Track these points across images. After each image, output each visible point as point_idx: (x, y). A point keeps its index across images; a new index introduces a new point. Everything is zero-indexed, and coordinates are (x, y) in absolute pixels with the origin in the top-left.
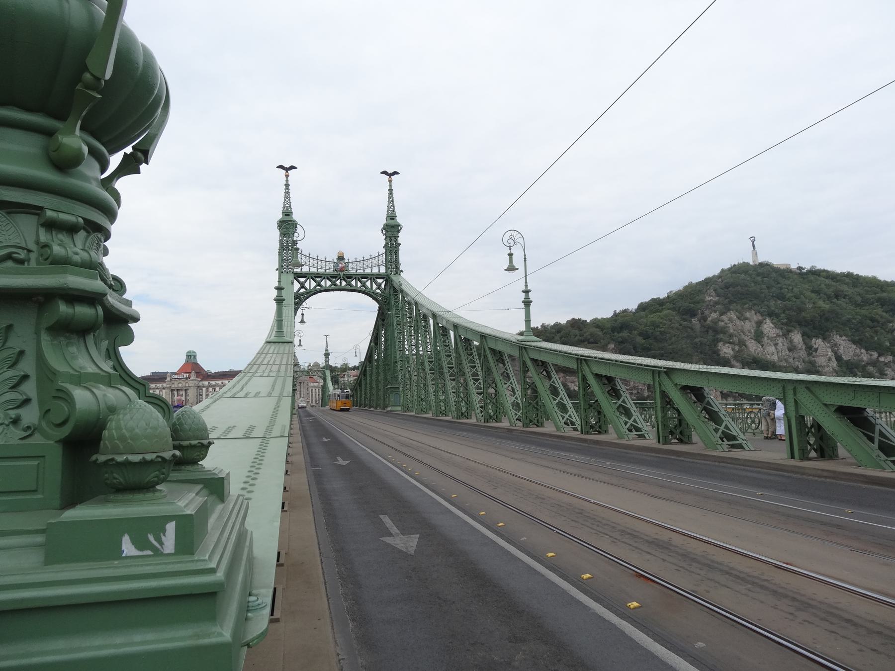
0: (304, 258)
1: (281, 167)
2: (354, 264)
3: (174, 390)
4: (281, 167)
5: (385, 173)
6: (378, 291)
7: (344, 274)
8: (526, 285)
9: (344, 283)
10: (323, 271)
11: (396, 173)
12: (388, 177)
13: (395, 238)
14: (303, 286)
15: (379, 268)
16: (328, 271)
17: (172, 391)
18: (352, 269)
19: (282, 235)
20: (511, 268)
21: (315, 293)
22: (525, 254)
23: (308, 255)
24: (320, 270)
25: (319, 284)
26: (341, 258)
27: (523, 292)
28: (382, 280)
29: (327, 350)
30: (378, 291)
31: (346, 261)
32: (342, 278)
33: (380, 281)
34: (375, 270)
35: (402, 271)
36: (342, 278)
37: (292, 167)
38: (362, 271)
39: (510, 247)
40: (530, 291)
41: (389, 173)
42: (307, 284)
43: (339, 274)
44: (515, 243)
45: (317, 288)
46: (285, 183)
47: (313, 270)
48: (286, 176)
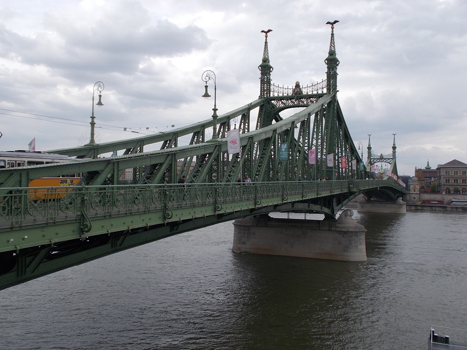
1: (263, 31)
4: (263, 31)
7: (297, 96)
8: (215, 106)
10: (286, 95)
11: (336, 22)
12: (331, 25)
16: (289, 95)
18: (305, 92)
20: (206, 95)
22: (215, 85)
24: (285, 95)
26: (298, 86)
27: (213, 110)
29: (394, 145)
31: (301, 87)
34: (320, 92)
35: (338, 91)
37: (269, 31)
38: (311, 93)
39: (206, 82)
40: (217, 110)
41: (331, 22)
43: (294, 96)
44: (209, 78)
46: (265, 41)
48: (266, 36)
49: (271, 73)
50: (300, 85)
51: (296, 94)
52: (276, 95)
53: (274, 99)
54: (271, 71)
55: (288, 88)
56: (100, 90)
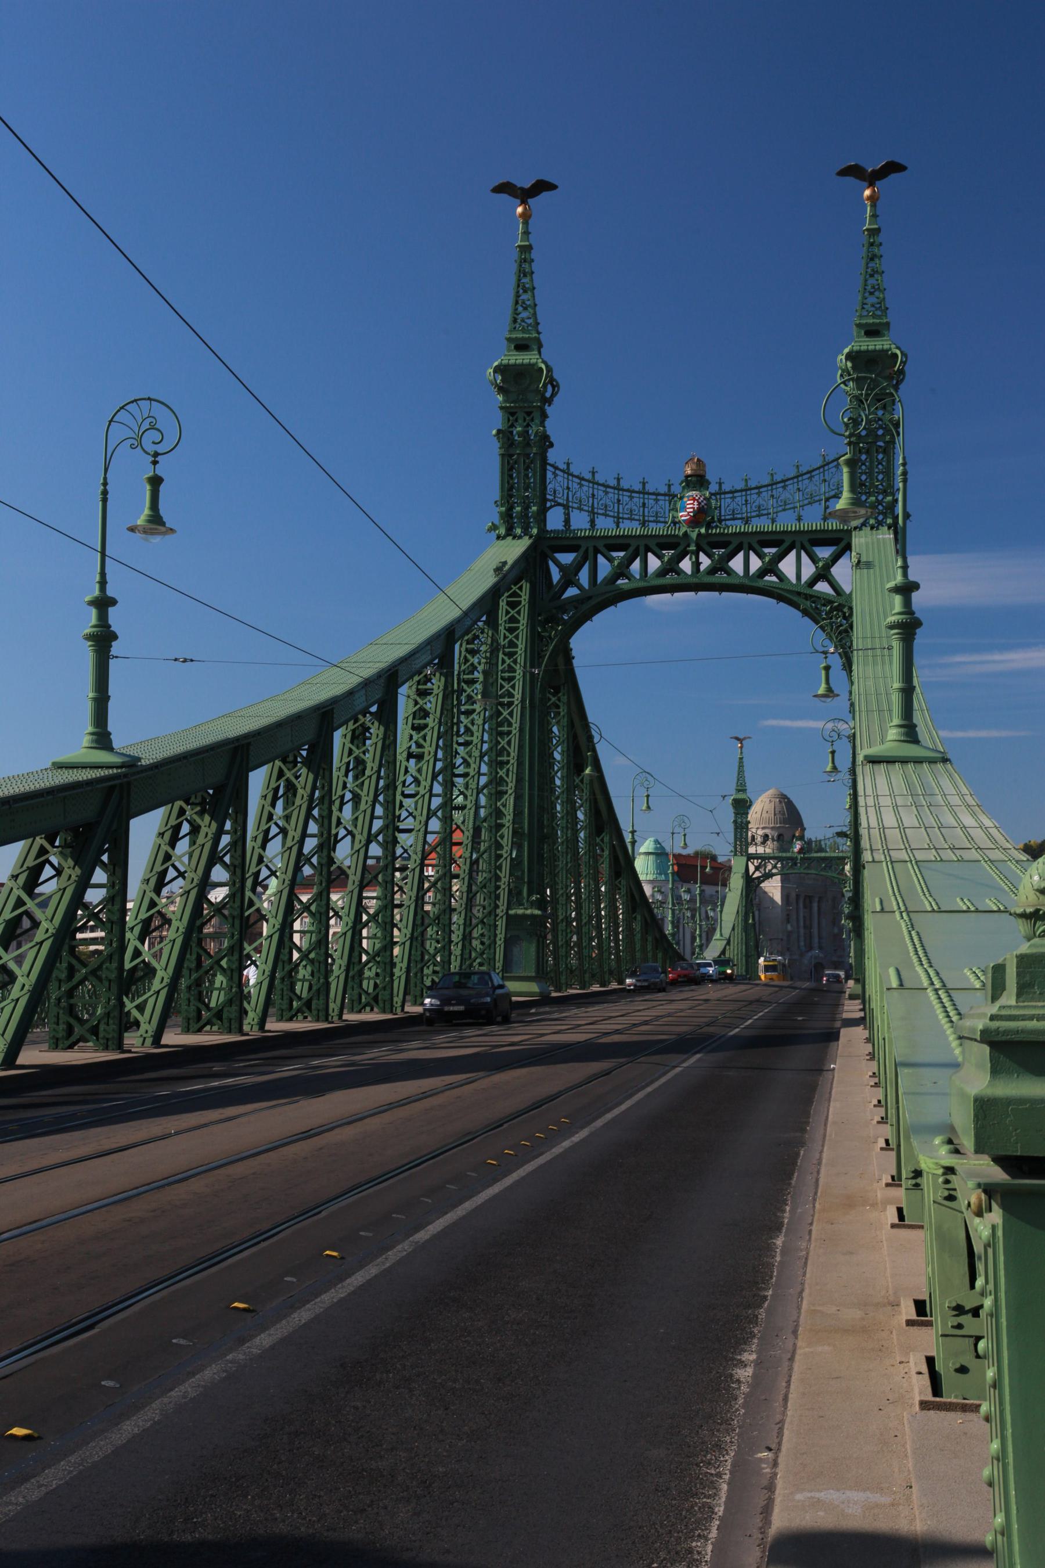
0: (574, 485)
5: (853, 171)
6: (822, 587)
7: (699, 535)
9: (705, 562)
14: (570, 577)
23: (589, 476)
25: (622, 571)
31: (714, 488)
33: (824, 553)
37: (542, 186)
42: (584, 576)
43: (686, 534)
47: (605, 526)
49: (549, 410)
50: (708, 477)
51: (695, 521)
52: (580, 521)
53: (567, 542)
54: (549, 401)
55: (643, 492)
56: (151, 448)
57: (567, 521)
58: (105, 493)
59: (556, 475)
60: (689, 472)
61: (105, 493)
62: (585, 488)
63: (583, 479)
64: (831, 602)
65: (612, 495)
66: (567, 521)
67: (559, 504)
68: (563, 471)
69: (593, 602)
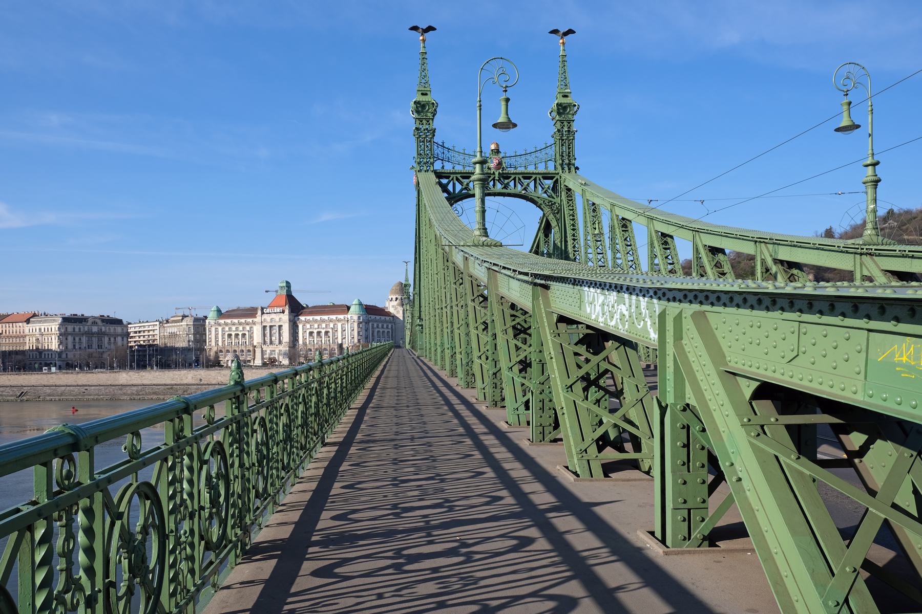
0: (446, 152)
2: (513, 160)
3: (266, 326)
7: (499, 173)
13: (569, 123)
15: (546, 164)
17: (264, 327)
19: (418, 122)
21: (461, 199)
28: (551, 181)
30: (545, 195)
32: (497, 178)
34: (541, 169)
35: (577, 168)
36: (497, 178)
37: (430, 29)
42: (450, 187)
43: (494, 173)
45: (463, 192)
47: (459, 168)
52: (448, 167)
57: (443, 167)
58: (480, 106)
59: (438, 147)
60: (493, 148)
61: (480, 106)
62: (450, 153)
63: (449, 149)
64: (551, 201)
65: (462, 157)
66: (443, 167)
67: (440, 159)
68: (441, 146)
69: (457, 199)
